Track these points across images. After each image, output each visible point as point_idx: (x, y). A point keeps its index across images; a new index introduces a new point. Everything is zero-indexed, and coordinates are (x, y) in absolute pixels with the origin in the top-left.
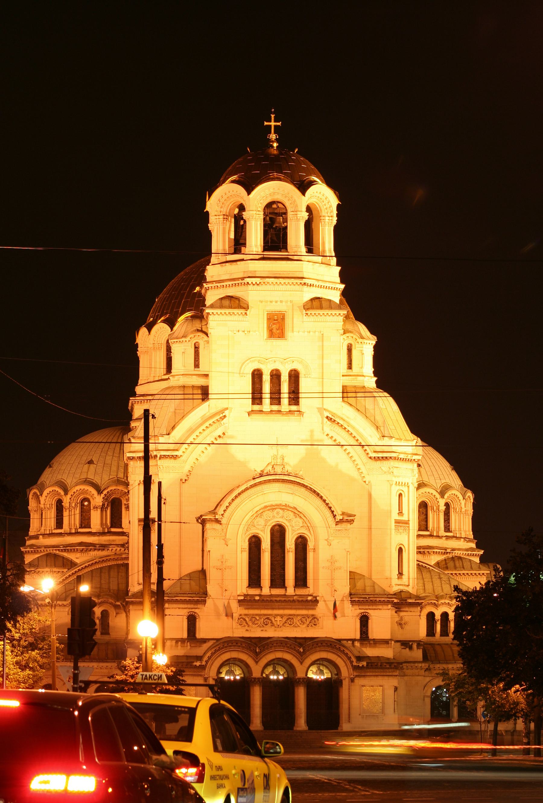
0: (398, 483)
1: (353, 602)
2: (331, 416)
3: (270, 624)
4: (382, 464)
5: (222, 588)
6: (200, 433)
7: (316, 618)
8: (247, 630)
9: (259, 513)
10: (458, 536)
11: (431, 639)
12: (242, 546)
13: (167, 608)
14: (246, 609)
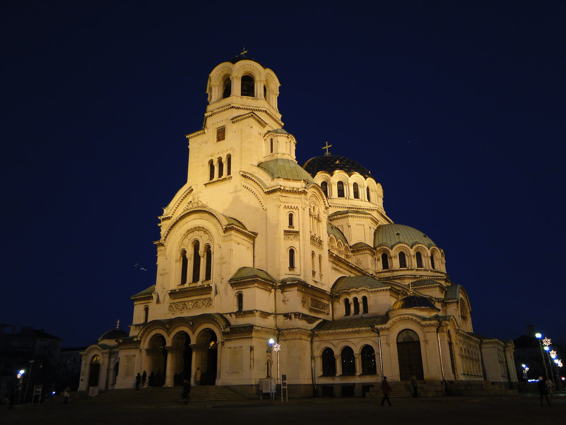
0: (287, 206)
1: (232, 285)
2: (243, 174)
3: (185, 308)
4: (273, 195)
5: (162, 287)
6: (180, 202)
7: (211, 300)
8: (173, 314)
9: (186, 235)
10: (427, 269)
11: (347, 317)
12: (176, 258)
13: (135, 305)
14: (174, 299)
